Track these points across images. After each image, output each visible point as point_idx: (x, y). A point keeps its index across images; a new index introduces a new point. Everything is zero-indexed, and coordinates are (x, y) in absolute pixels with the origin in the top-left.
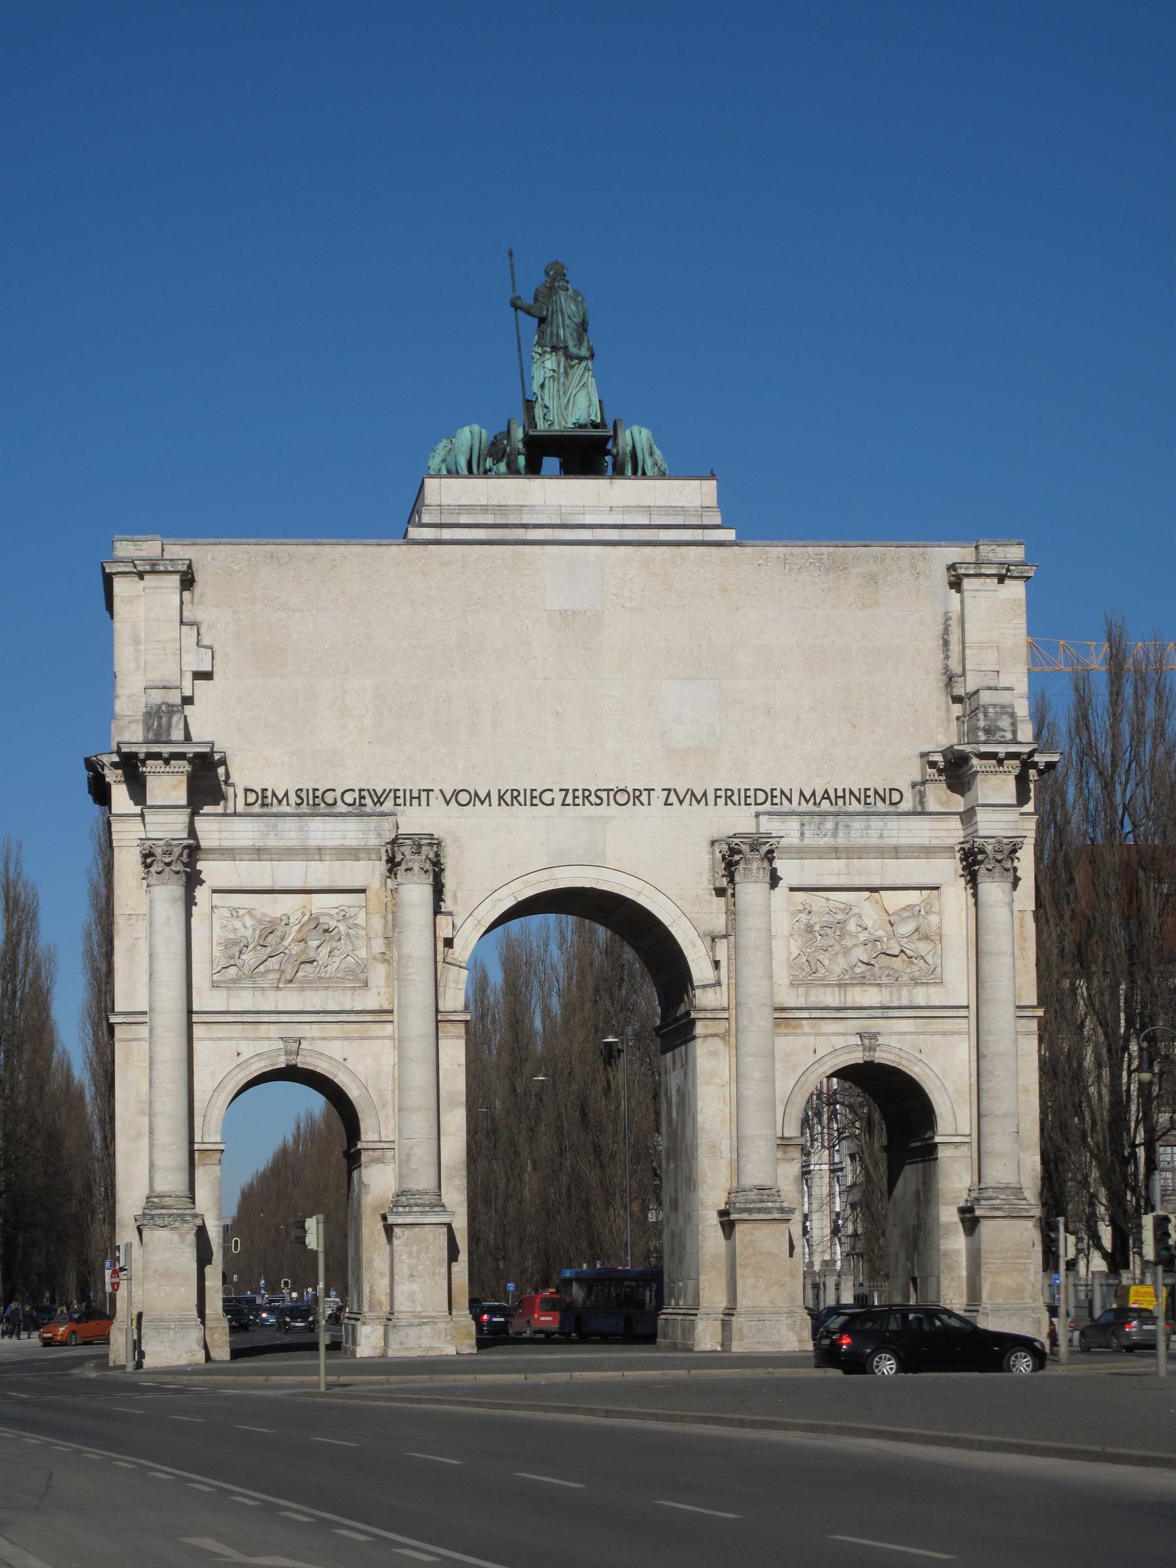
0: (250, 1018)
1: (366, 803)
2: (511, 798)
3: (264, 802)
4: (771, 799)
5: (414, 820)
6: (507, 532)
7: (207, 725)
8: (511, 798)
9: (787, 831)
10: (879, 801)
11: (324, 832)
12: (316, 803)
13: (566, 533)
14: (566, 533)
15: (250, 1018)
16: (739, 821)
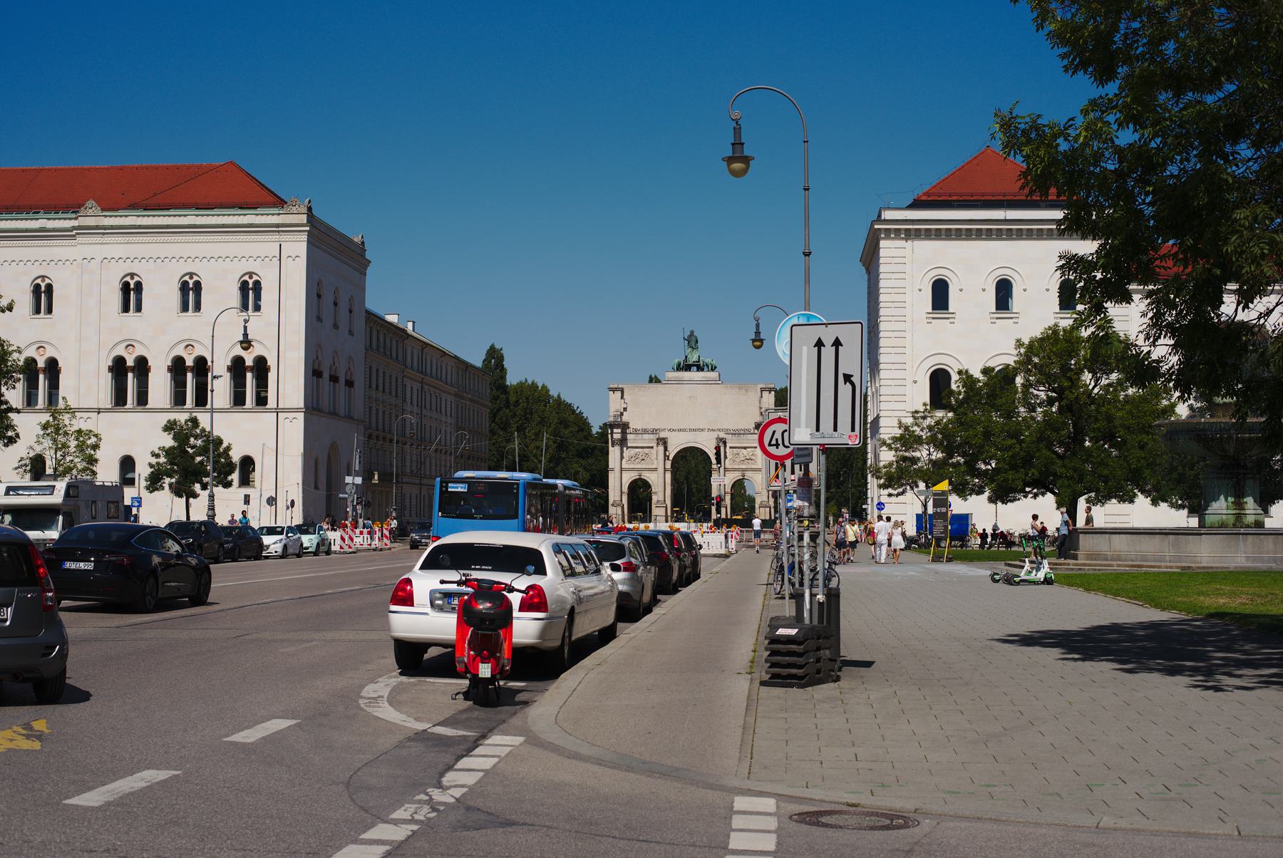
0: (633, 470)
1: (654, 431)
2: (680, 430)
3: (636, 432)
4: (727, 432)
5: (662, 435)
6: (680, 382)
7: (625, 418)
8: (680, 430)
9: (728, 437)
10: (746, 432)
11: (646, 436)
12: (645, 431)
13: (691, 382)
14: (691, 382)
15: (633, 470)
16: (722, 435)
